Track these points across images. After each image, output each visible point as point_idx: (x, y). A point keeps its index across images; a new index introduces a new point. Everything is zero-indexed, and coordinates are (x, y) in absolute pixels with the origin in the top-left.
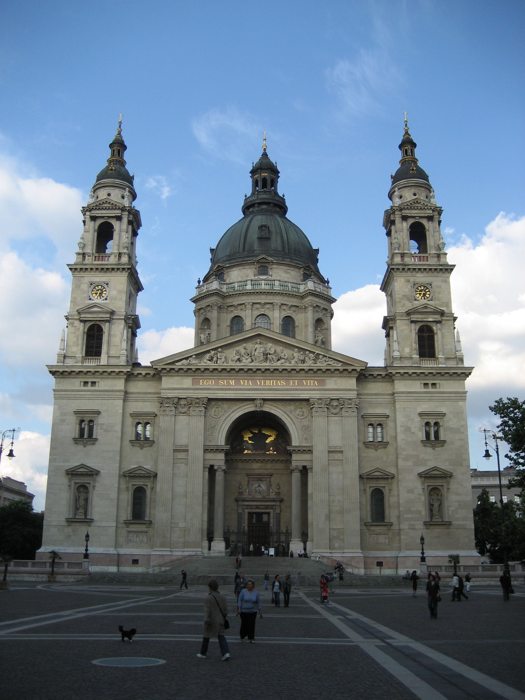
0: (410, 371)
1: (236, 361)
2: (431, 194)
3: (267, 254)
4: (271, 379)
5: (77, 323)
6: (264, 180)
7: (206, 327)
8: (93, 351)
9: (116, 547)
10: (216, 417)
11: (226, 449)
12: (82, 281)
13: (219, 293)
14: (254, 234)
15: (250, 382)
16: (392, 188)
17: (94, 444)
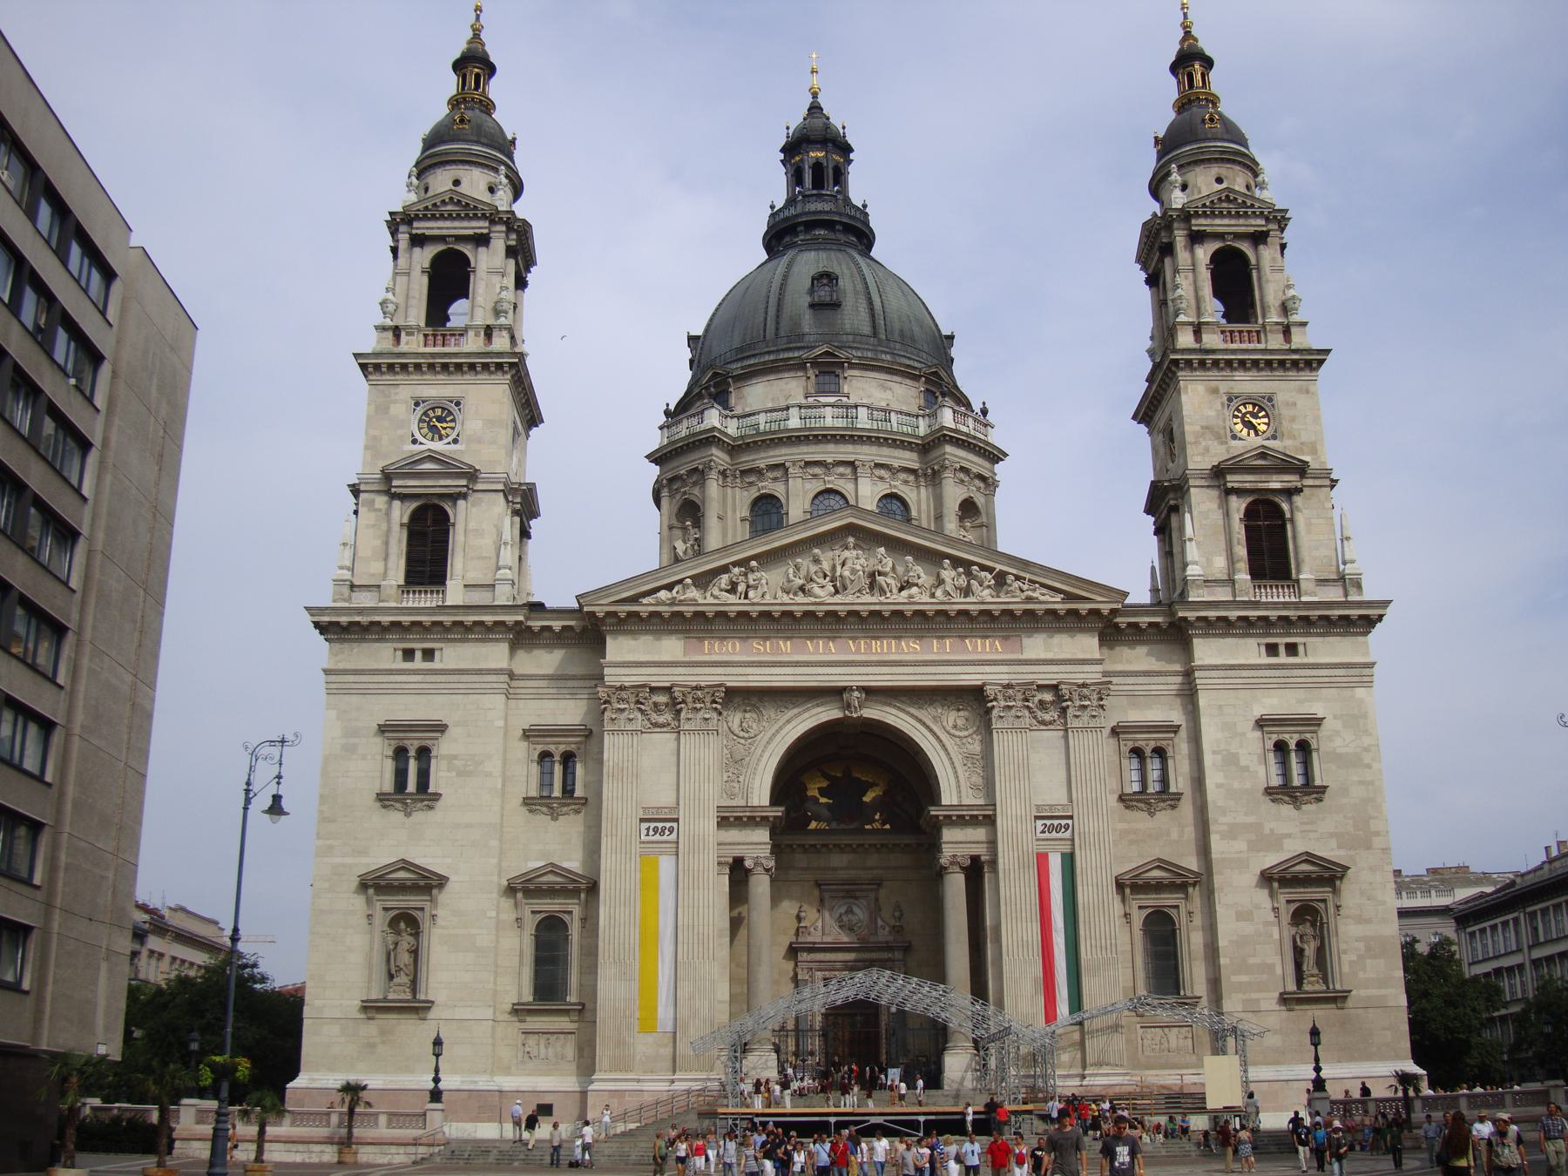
0: (1233, 614)
1: (795, 594)
2: (1260, 179)
3: (836, 344)
4: (885, 637)
5: (381, 501)
6: (818, 167)
7: (688, 523)
8: (420, 572)
10: (746, 735)
11: (775, 817)
12: (393, 398)
13: (719, 439)
14: (799, 296)
15: (831, 644)
16: (1160, 167)
17: (431, 808)
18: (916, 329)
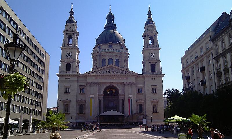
5: (64, 62)
9: (76, 120)
18: (120, 39)
